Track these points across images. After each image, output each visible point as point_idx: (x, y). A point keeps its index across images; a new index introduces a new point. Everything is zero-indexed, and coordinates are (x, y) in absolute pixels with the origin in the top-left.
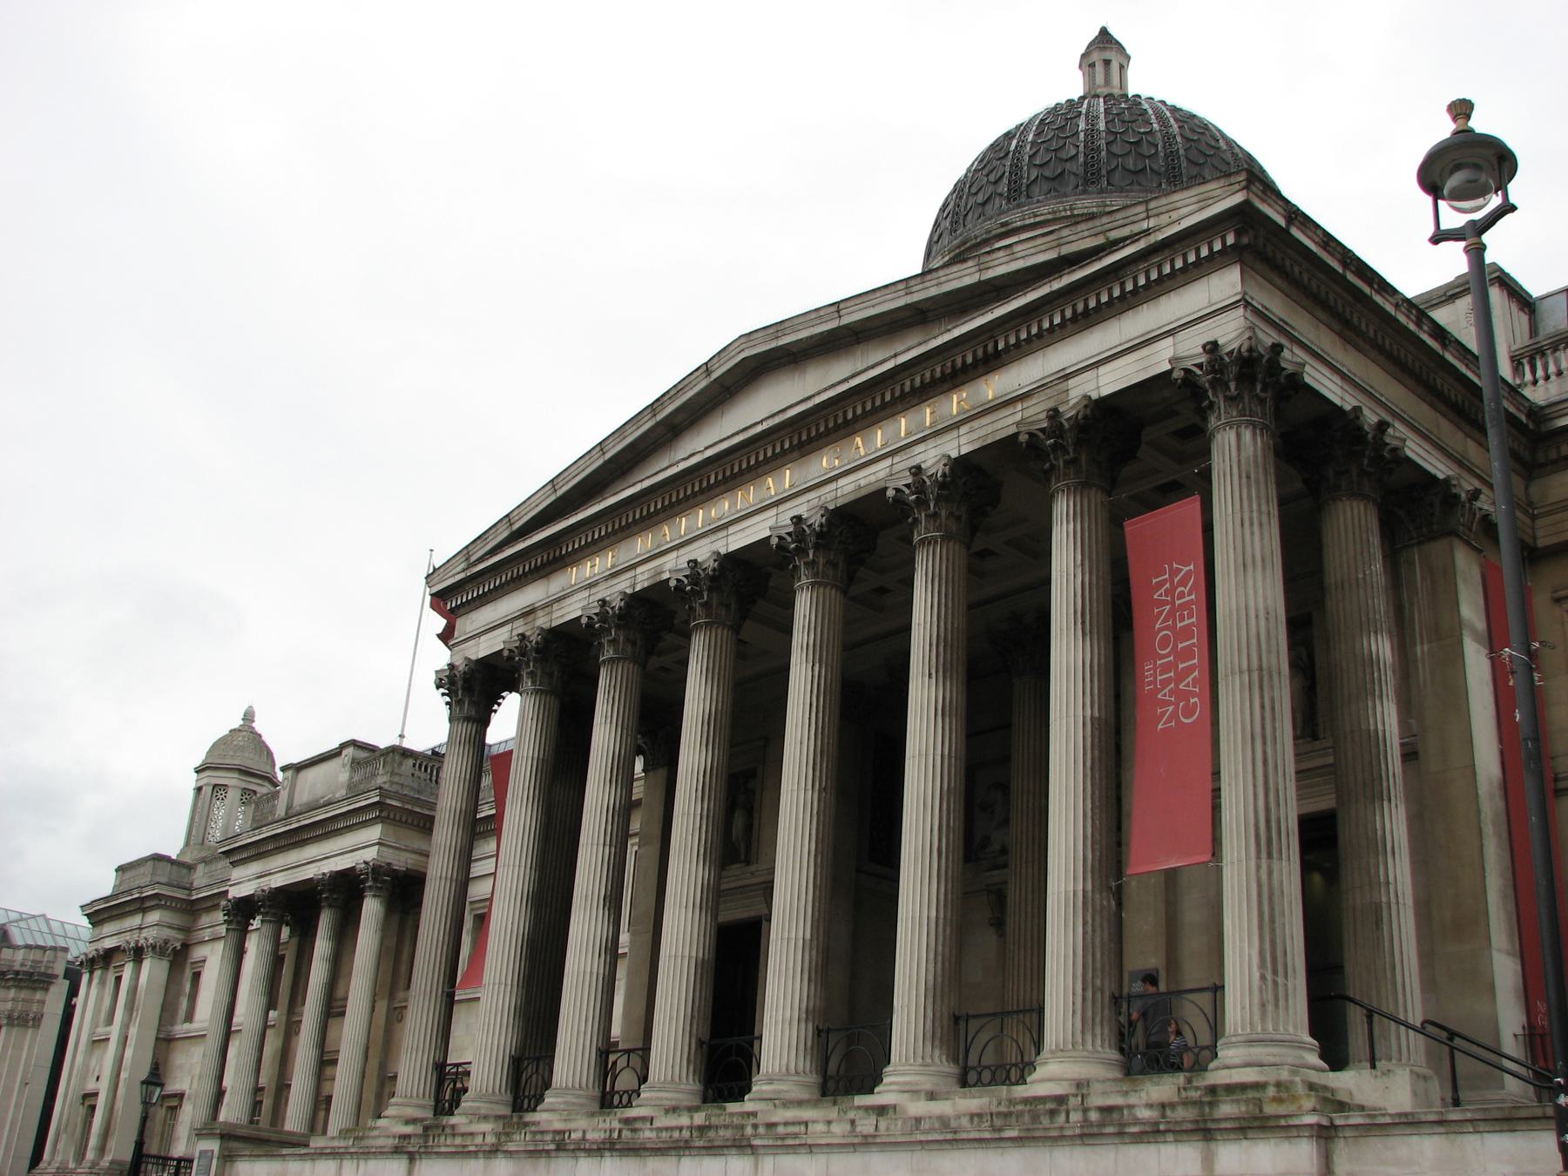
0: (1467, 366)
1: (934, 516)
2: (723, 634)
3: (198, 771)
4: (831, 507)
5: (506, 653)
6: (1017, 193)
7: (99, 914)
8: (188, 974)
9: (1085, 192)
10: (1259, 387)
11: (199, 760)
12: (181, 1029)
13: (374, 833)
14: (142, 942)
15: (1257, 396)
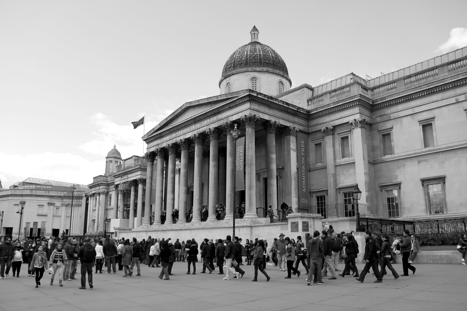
0: (293, 107)
1: (212, 136)
2: (186, 151)
3: (106, 158)
4: (199, 133)
5: (155, 151)
6: (235, 67)
7: (91, 187)
8: (109, 197)
9: (245, 67)
10: (252, 121)
11: (106, 156)
12: (109, 207)
13: (139, 173)
14: (100, 192)
15: (252, 123)
